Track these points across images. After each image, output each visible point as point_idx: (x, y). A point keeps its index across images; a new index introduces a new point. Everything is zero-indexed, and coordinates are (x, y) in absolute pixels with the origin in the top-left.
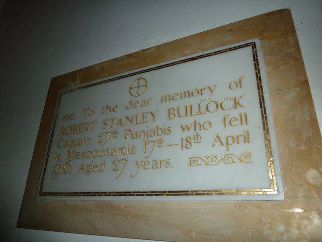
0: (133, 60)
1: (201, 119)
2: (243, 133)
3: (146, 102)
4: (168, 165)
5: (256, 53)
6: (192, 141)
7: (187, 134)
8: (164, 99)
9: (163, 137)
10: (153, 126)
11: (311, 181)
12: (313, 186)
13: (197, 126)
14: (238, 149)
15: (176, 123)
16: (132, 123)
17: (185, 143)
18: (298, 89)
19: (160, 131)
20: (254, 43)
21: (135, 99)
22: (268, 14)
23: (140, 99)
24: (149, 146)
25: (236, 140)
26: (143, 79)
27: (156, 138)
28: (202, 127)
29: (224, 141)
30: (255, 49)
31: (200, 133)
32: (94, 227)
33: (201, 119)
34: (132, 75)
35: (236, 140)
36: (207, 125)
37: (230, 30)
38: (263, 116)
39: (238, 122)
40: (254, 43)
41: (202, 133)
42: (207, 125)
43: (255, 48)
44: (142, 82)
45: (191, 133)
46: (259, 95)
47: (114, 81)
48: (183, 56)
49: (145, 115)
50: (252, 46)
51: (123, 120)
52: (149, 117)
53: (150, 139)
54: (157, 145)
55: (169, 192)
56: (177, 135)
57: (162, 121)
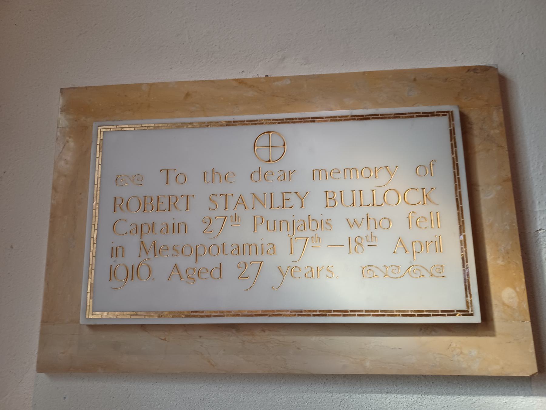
0: (251, 93)
1: (376, 213)
2: (434, 239)
3: (287, 175)
4: (330, 275)
5: (454, 129)
6: (365, 244)
7: (355, 232)
8: (317, 174)
9: (319, 232)
10: (302, 214)
11: (506, 301)
12: (508, 306)
13: (371, 222)
14: (428, 259)
15: (338, 215)
16: (264, 205)
17: (353, 244)
18: (499, 188)
19: (313, 225)
20: (452, 112)
21: (266, 167)
22: (469, 69)
23: (275, 168)
24: (298, 245)
25: (423, 246)
26: (279, 135)
27: (308, 233)
28: (378, 224)
29: (409, 246)
30: (452, 123)
31: (376, 233)
32: (209, 362)
33: (376, 213)
34: (255, 122)
35: (423, 246)
36: (385, 223)
37: (415, 80)
38: (459, 220)
39: (427, 224)
40: (452, 112)
41: (378, 233)
42: (385, 223)
43: (453, 120)
44: (276, 140)
45: (362, 232)
46: (456, 190)
47: (457, 221)
48: (343, 108)
49: (287, 196)
50: (449, 118)
51: (248, 199)
52: (294, 201)
53: (298, 234)
54: (309, 243)
55: (334, 311)
56: (342, 233)
57: (315, 208)
